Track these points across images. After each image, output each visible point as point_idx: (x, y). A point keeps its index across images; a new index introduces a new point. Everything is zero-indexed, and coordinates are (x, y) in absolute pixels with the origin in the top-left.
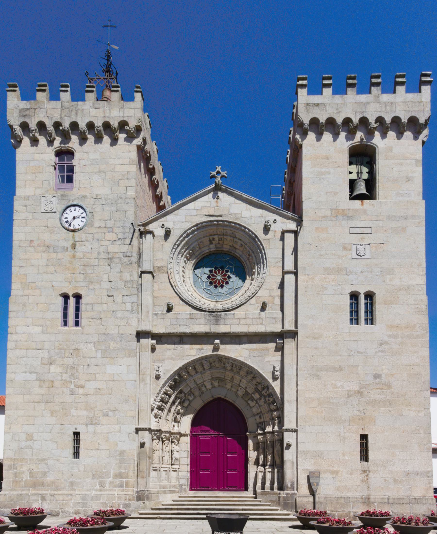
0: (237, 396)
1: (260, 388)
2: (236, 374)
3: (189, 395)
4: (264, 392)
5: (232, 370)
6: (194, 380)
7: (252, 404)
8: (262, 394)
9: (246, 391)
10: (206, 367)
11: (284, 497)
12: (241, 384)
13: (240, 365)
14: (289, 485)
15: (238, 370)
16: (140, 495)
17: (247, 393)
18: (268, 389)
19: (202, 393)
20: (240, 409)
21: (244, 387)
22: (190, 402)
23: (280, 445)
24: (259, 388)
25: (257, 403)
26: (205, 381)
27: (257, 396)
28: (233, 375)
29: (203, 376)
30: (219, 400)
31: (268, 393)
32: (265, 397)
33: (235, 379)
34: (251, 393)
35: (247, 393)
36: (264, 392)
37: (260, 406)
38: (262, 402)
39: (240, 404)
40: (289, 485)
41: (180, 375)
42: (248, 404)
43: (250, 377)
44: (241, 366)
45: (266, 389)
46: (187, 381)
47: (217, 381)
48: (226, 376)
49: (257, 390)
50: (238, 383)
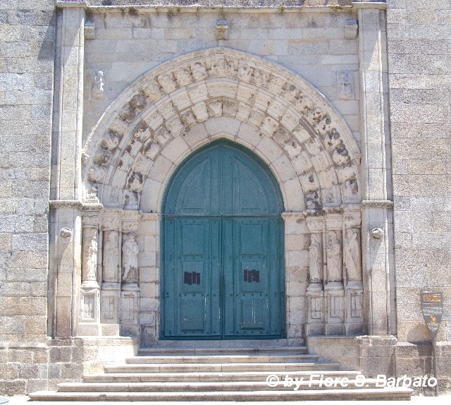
0: (261, 135)
1: (310, 118)
2: (261, 90)
3: (161, 133)
4: (319, 127)
5: (252, 82)
6: (171, 101)
7: (292, 151)
8: (314, 131)
9: (281, 125)
10: (197, 76)
11: (369, 350)
12: (269, 111)
13: (269, 72)
14: (379, 322)
15: (265, 83)
16: (59, 350)
17: (281, 130)
18: (328, 121)
19: (188, 129)
20: (268, 162)
21: (276, 116)
22: (162, 148)
23: (357, 238)
24: (308, 119)
25: (304, 149)
26: (193, 105)
27: (303, 135)
28: (253, 92)
29: (191, 95)
30: (222, 145)
31: (327, 129)
32: (322, 138)
33: (256, 100)
34: (291, 129)
35: (281, 130)
36: (319, 127)
37: (310, 156)
38: (314, 148)
39: (266, 151)
40: (379, 322)
41: (143, 92)
42: (285, 153)
43: (291, 95)
44: (271, 75)
45: (324, 122)
46: (156, 104)
47: (220, 104)
48: (239, 93)
49: (303, 123)
50: (264, 109)
